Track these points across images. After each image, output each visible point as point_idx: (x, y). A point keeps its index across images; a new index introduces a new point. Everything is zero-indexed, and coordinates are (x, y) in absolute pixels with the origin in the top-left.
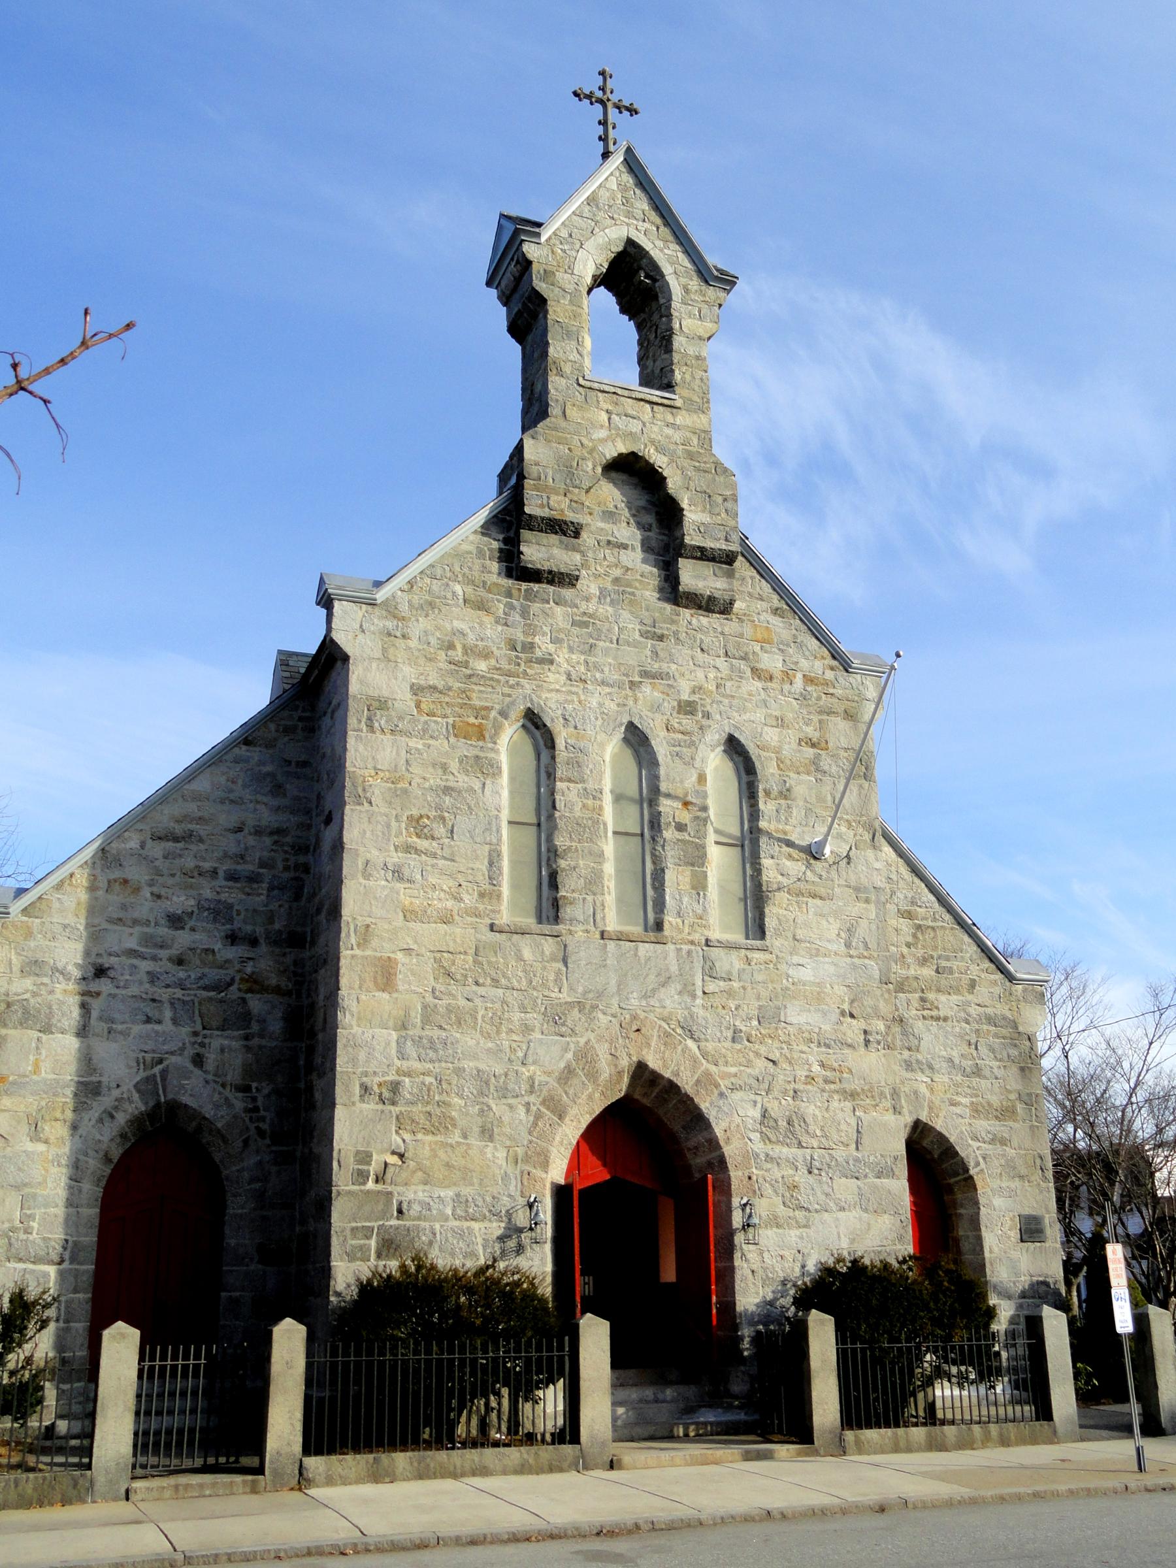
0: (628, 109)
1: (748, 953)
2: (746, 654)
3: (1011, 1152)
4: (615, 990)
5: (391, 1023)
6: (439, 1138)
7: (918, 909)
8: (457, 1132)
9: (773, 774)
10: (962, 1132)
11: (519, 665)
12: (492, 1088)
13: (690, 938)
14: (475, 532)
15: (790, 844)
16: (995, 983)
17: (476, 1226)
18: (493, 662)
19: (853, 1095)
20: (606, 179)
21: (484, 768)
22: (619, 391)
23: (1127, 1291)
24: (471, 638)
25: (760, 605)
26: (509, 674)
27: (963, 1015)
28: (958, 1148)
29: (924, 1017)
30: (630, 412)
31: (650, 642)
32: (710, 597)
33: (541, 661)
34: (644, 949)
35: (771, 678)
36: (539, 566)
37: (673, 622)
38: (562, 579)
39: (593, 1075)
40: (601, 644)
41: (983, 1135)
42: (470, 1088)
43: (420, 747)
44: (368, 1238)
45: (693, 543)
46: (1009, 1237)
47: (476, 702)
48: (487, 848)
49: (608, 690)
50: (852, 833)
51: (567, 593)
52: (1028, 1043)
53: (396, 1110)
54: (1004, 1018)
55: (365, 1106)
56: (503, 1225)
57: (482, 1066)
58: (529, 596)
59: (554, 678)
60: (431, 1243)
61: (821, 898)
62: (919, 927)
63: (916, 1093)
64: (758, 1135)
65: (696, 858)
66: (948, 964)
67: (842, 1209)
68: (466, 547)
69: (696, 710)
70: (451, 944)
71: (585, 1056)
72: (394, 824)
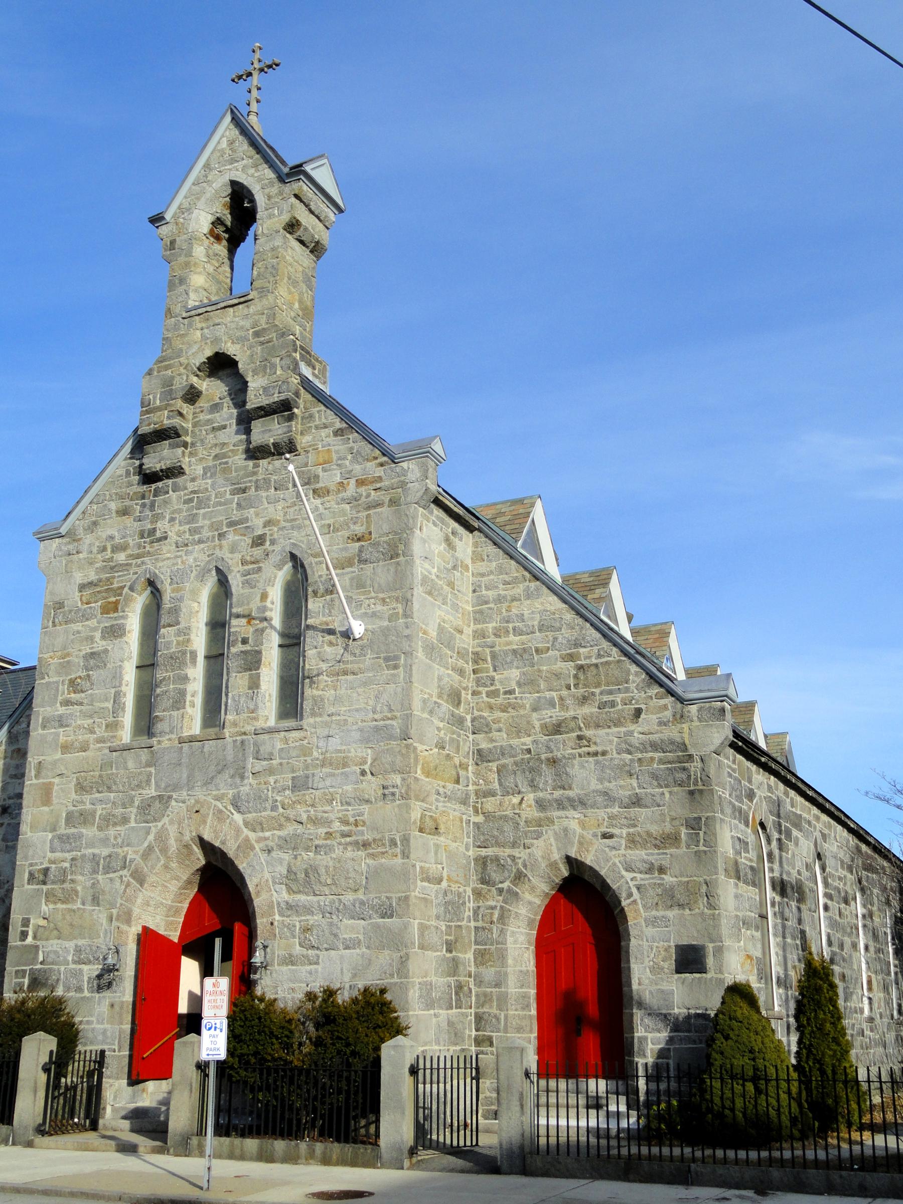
0: (270, 67)
1: (286, 733)
2: (309, 479)
3: (668, 879)
4: (185, 782)
5: (48, 828)
6: (69, 906)
7: (582, 650)
8: (79, 901)
9: (320, 576)
10: (614, 864)
11: (145, 547)
12: (101, 867)
13: (243, 730)
14: (126, 459)
15: (331, 632)
16: (665, 707)
17: (85, 968)
18: (129, 552)
19: (365, 845)
20: (219, 142)
21: (115, 632)
22: (209, 309)
23: (225, 1022)
24: (117, 540)
25: (324, 433)
26: (138, 556)
27: (624, 746)
28: (609, 881)
29: (580, 756)
30: (217, 321)
31: (236, 497)
32: (273, 444)
33: (159, 540)
34: (209, 746)
35: (328, 492)
36: (154, 470)
37: (255, 473)
38: (174, 472)
39: (164, 850)
40: (202, 511)
41: (639, 865)
42: (88, 867)
43: (80, 628)
44: (24, 977)
45: (253, 406)
46: (663, 969)
47: (115, 585)
48: (113, 691)
49: (202, 546)
50: (385, 608)
51: (180, 480)
52: (700, 765)
53: (45, 887)
54: (672, 742)
55: (30, 887)
56: (101, 967)
57: (96, 851)
58: (156, 493)
59: (167, 549)
60: (58, 980)
61: (354, 674)
62: (581, 668)
63: (566, 830)
64: (284, 887)
65: (253, 662)
66: (611, 698)
67: (347, 948)
68: (119, 472)
69: (265, 541)
70: (86, 766)
71: (161, 837)
72: (61, 687)
